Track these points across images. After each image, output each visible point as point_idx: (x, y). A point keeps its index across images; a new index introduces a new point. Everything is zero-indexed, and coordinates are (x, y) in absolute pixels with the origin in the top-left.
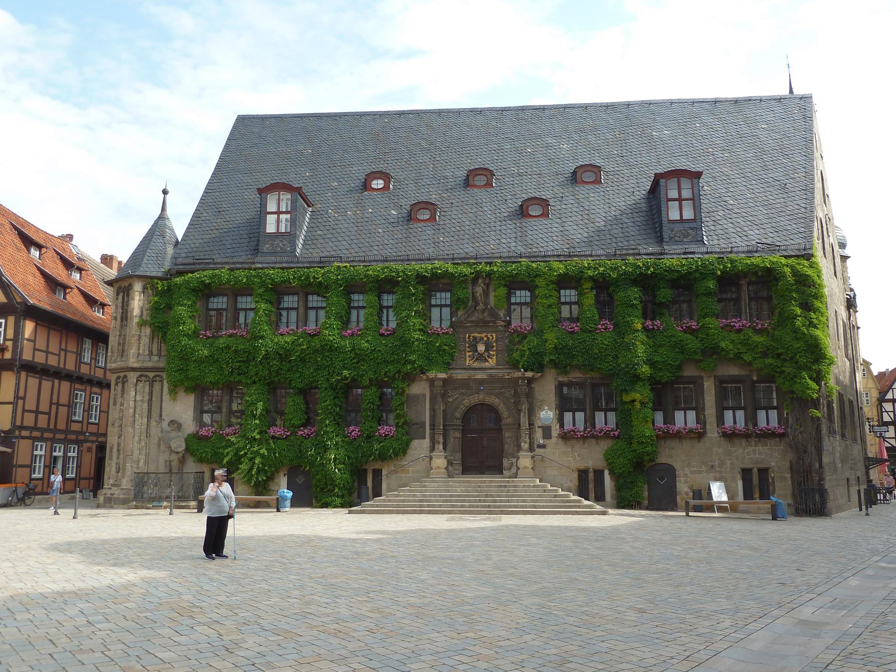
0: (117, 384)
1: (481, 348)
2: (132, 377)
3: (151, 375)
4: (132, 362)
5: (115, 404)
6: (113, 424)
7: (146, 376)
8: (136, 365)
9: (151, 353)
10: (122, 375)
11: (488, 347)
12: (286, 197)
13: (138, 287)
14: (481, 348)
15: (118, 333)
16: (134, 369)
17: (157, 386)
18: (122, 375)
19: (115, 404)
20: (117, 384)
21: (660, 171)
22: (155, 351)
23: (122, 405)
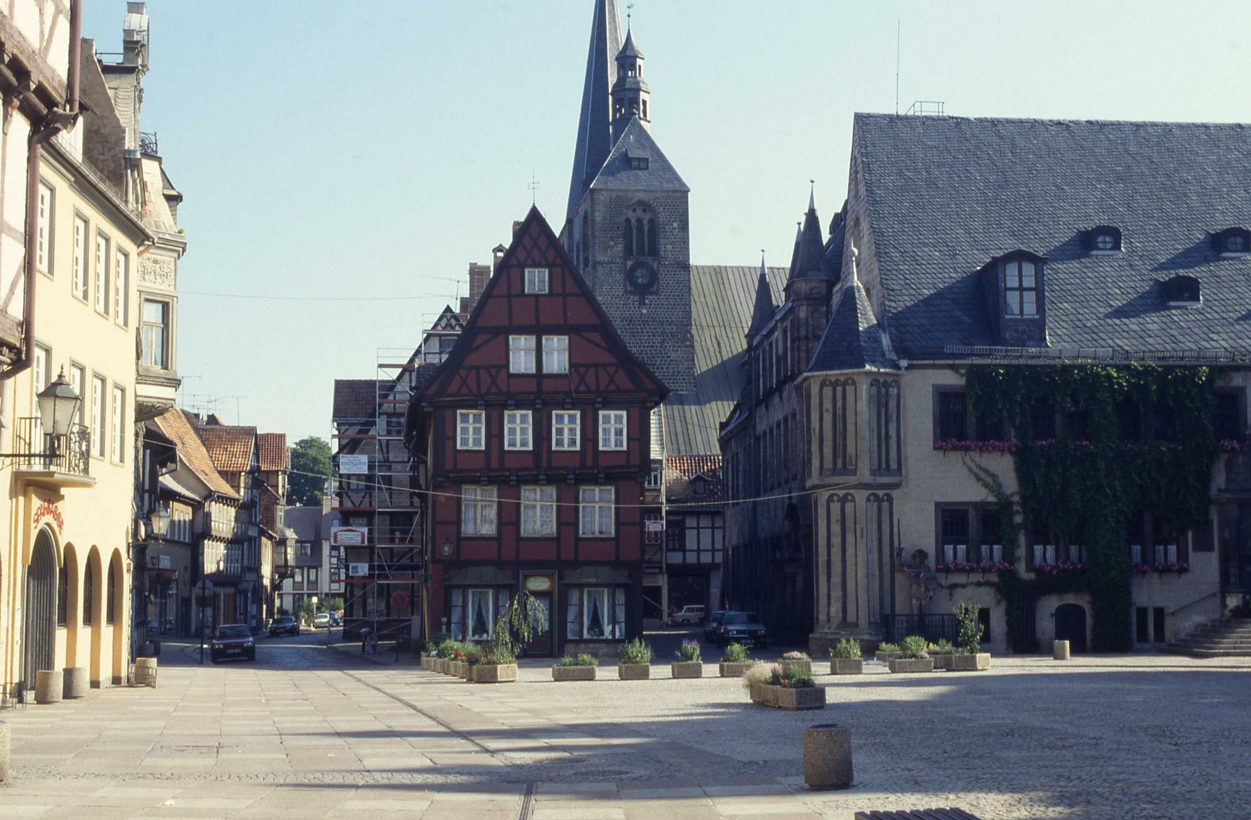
3: (881, 493)
7: (876, 496)
10: (841, 493)
12: (1029, 269)
17: (885, 505)
22: (884, 466)
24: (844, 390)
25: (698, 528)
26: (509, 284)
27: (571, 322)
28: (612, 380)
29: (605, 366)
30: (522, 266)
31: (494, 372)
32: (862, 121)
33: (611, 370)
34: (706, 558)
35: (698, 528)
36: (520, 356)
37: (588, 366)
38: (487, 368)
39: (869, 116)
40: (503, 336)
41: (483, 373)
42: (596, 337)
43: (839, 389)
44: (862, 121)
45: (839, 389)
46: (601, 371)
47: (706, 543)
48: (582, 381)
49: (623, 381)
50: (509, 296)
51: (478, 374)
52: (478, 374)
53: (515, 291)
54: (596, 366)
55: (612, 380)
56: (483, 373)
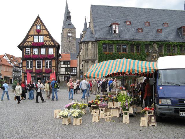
0: (85, 63)
1: (154, 57)
2: (90, 61)
3: (93, 61)
4: (90, 59)
5: (85, 67)
6: (85, 71)
8: (91, 59)
9: (93, 57)
11: (156, 57)
12: (117, 26)
13: (90, 43)
14: (154, 57)
15: (85, 52)
16: (91, 60)
18: (87, 61)
19: (85, 67)
20: (85, 63)
21: (182, 26)
23: (87, 67)
24: (87, 45)
25: (75, 69)
26: (34, 28)
27: (44, 34)
28: (50, 43)
29: (49, 41)
30: (36, 25)
31: (31, 42)
32: (92, 6)
33: (50, 42)
34: (76, 73)
35: (75, 69)
36: (36, 40)
37: (46, 41)
38: (30, 41)
39: (95, 6)
40: (33, 36)
41: (30, 42)
42: (48, 36)
43: (86, 44)
44: (92, 6)
45: (86, 44)
46: (49, 42)
47: (76, 71)
48: (46, 43)
49: (52, 43)
50: (34, 30)
51: (29, 43)
52: (29, 43)
53: (35, 29)
54: (48, 41)
55: (50, 43)
56: (30, 42)
